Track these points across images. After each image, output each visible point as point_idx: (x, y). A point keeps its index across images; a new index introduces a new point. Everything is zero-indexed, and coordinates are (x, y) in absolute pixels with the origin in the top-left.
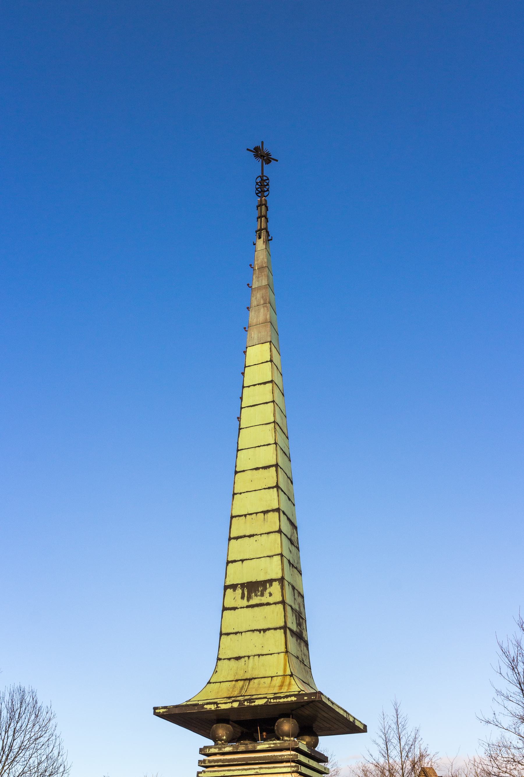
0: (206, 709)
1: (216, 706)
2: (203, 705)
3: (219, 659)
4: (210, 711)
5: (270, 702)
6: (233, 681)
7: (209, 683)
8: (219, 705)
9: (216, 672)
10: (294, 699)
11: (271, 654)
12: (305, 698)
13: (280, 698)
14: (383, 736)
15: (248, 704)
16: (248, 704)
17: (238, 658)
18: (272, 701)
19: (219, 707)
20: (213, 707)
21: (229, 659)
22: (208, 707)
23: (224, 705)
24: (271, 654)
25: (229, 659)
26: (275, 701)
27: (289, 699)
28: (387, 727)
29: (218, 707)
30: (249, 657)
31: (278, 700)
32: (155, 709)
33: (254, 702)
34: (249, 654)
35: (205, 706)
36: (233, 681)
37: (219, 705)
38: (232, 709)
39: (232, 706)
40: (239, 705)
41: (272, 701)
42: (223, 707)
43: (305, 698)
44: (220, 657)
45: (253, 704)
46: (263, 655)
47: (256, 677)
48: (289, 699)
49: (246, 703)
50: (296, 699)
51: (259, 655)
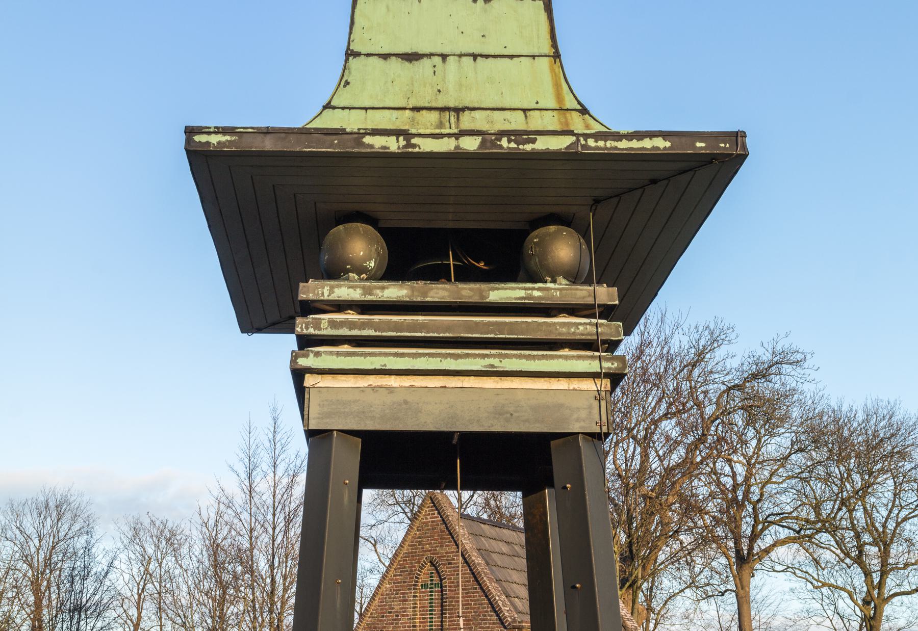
0: (372, 146)
1: (402, 142)
2: (360, 134)
3: (350, 54)
4: (385, 156)
5: (585, 147)
6: (405, 109)
7: (328, 106)
8: (414, 141)
9: (347, 83)
10: (661, 143)
11: (511, 57)
12: (699, 145)
13: (618, 137)
14: (247, 461)
15: (513, 145)
16: (513, 145)
17: (411, 57)
18: (591, 142)
19: (414, 146)
20: (393, 144)
21: (385, 57)
22: (377, 142)
23: (429, 140)
24: (511, 57)
25: (385, 57)
26: (601, 144)
27: (647, 144)
28: (254, 447)
29: (409, 145)
30: (444, 57)
31: (610, 144)
32: (190, 131)
33: (534, 141)
34: (446, 51)
35: (368, 140)
36: (405, 109)
37: (414, 141)
38: (459, 156)
39: (457, 147)
40: (480, 147)
41: (591, 142)
42: (428, 146)
43: (699, 145)
44: (355, 47)
45: (528, 147)
46: (487, 56)
47: (476, 105)
48: (647, 144)
49: (504, 142)
50: (668, 144)
51: (475, 57)
